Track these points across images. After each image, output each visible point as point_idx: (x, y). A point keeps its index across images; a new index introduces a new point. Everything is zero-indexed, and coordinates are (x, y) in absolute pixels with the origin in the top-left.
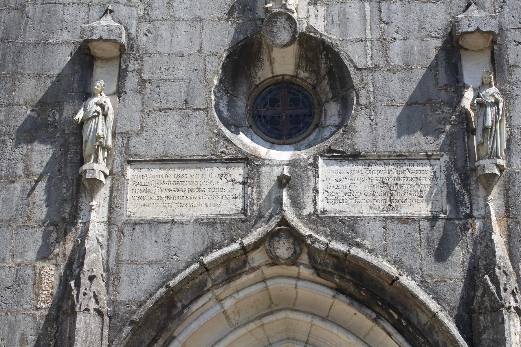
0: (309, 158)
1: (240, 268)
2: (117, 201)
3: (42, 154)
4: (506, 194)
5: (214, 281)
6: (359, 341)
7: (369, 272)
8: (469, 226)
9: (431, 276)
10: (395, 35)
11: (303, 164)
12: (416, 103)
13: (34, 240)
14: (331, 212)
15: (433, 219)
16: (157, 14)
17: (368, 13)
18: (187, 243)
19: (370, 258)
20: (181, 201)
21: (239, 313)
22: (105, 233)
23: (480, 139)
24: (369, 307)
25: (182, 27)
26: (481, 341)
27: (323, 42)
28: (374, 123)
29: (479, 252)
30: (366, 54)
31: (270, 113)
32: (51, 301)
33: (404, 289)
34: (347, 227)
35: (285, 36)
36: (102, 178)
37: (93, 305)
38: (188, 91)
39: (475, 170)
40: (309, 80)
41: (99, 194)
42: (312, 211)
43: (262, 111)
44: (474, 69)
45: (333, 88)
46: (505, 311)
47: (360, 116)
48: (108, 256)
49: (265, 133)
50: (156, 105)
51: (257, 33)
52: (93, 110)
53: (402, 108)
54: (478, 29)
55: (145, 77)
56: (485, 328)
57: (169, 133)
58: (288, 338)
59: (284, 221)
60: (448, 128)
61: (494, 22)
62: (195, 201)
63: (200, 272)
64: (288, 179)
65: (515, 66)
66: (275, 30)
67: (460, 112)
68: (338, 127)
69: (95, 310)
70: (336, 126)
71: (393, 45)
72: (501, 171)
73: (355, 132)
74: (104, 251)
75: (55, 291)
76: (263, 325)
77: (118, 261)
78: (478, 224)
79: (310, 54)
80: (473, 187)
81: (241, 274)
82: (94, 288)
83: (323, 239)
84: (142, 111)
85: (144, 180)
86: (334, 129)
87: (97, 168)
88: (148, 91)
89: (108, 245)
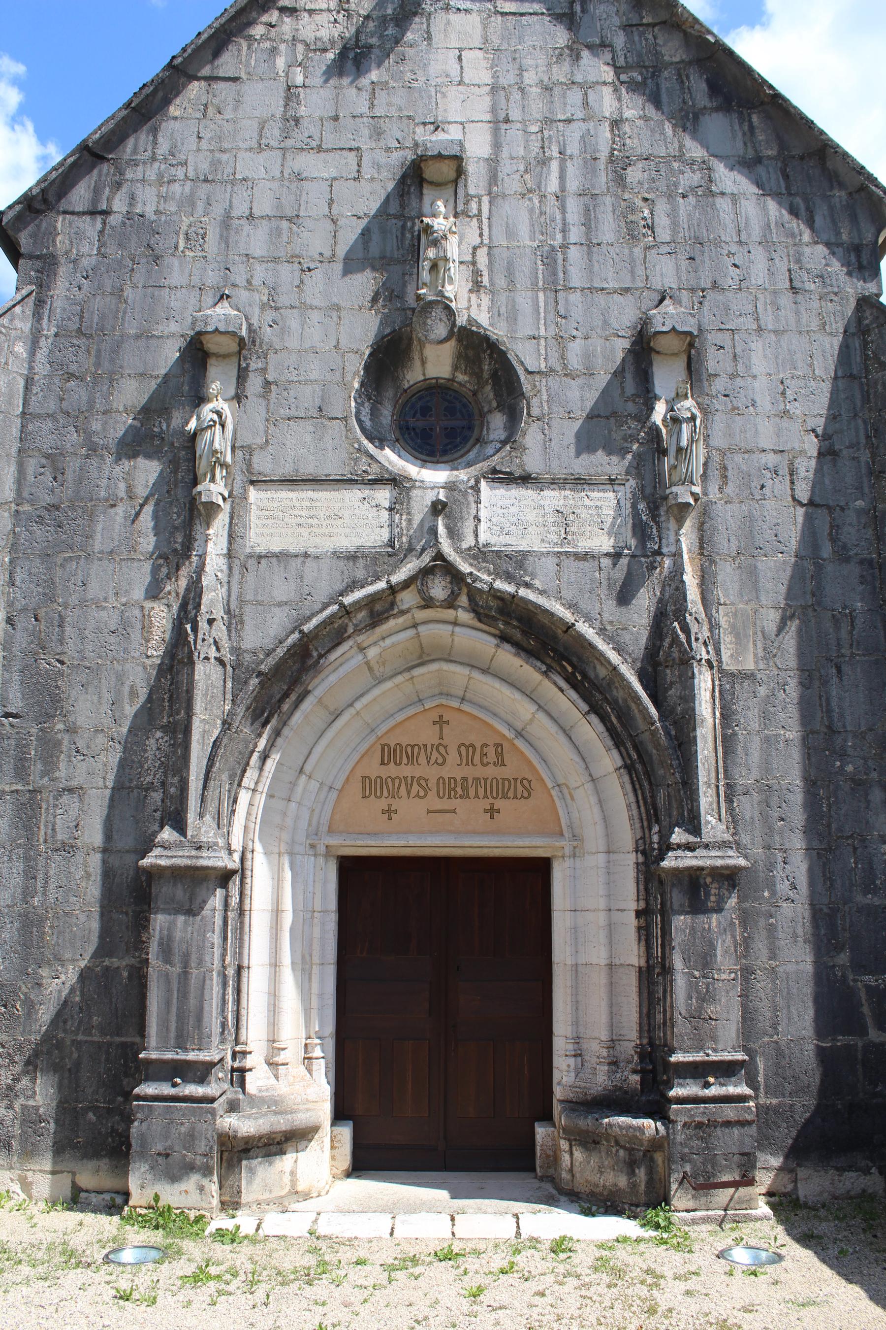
0: (469, 480)
1: (387, 611)
2: (239, 530)
3: (147, 471)
4: (701, 528)
5: (356, 626)
6: (525, 698)
7: (540, 617)
8: (656, 564)
9: (611, 622)
10: (575, 333)
11: (462, 487)
12: (599, 416)
14: (495, 545)
15: (616, 556)
16: (283, 300)
17: (542, 304)
18: (324, 582)
19: (541, 601)
20: (314, 530)
21: (384, 664)
22: (225, 568)
23: (673, 461)
24: (538, 658)
25: (315, 316)
26: (666, 698)
27: (487, 338)
29: (667, 595)
30: (539, 355)
31: (420, 424)
32: (163, 648)
33: (581, 638)
34: (514, 563)
35: (441, 330)
36: (221, 502)
37: (213, 653)
38: (322, 396)
40: (468, 385)
41: (216, 521)
42: (473, 544)
43: (412, 422)
44: (667, 377)
46: (695, 664)
47: (531, 430)
48: (229, 596)
49: (414, 449)
51: (407, 326)
52: (208, 419)
53: (581, 421)
54: (674, 329)
55: (270, 379)
56: (672, 683)
57: (299, 447)
58: (441, 694)
59: (439, 556)
60: (635, 447)
61: (693, 321)
62: (332, 530)
63: (340, 615)
64: (444, 505)
65: (715, 375)
66: (429, 322)
67: (650, 428)
68: (504, 443)
69: (216, 658)
70: (501, 442)
71: (571, 344)
72: (696, 500)
73: (525, 449)
74: (225, 589)
75: (167, 636)
76: (412, 678)
77: (241, 601)
78: (667, 562)
80: (662, 519)
81: (388, 618)
82: (214, 633)
83: (485, 577)
84: (267, 420)
85: (270, 505)
86: (499, 445)
87: (214, 489)
88: (273, 395)
89: (229, 582)
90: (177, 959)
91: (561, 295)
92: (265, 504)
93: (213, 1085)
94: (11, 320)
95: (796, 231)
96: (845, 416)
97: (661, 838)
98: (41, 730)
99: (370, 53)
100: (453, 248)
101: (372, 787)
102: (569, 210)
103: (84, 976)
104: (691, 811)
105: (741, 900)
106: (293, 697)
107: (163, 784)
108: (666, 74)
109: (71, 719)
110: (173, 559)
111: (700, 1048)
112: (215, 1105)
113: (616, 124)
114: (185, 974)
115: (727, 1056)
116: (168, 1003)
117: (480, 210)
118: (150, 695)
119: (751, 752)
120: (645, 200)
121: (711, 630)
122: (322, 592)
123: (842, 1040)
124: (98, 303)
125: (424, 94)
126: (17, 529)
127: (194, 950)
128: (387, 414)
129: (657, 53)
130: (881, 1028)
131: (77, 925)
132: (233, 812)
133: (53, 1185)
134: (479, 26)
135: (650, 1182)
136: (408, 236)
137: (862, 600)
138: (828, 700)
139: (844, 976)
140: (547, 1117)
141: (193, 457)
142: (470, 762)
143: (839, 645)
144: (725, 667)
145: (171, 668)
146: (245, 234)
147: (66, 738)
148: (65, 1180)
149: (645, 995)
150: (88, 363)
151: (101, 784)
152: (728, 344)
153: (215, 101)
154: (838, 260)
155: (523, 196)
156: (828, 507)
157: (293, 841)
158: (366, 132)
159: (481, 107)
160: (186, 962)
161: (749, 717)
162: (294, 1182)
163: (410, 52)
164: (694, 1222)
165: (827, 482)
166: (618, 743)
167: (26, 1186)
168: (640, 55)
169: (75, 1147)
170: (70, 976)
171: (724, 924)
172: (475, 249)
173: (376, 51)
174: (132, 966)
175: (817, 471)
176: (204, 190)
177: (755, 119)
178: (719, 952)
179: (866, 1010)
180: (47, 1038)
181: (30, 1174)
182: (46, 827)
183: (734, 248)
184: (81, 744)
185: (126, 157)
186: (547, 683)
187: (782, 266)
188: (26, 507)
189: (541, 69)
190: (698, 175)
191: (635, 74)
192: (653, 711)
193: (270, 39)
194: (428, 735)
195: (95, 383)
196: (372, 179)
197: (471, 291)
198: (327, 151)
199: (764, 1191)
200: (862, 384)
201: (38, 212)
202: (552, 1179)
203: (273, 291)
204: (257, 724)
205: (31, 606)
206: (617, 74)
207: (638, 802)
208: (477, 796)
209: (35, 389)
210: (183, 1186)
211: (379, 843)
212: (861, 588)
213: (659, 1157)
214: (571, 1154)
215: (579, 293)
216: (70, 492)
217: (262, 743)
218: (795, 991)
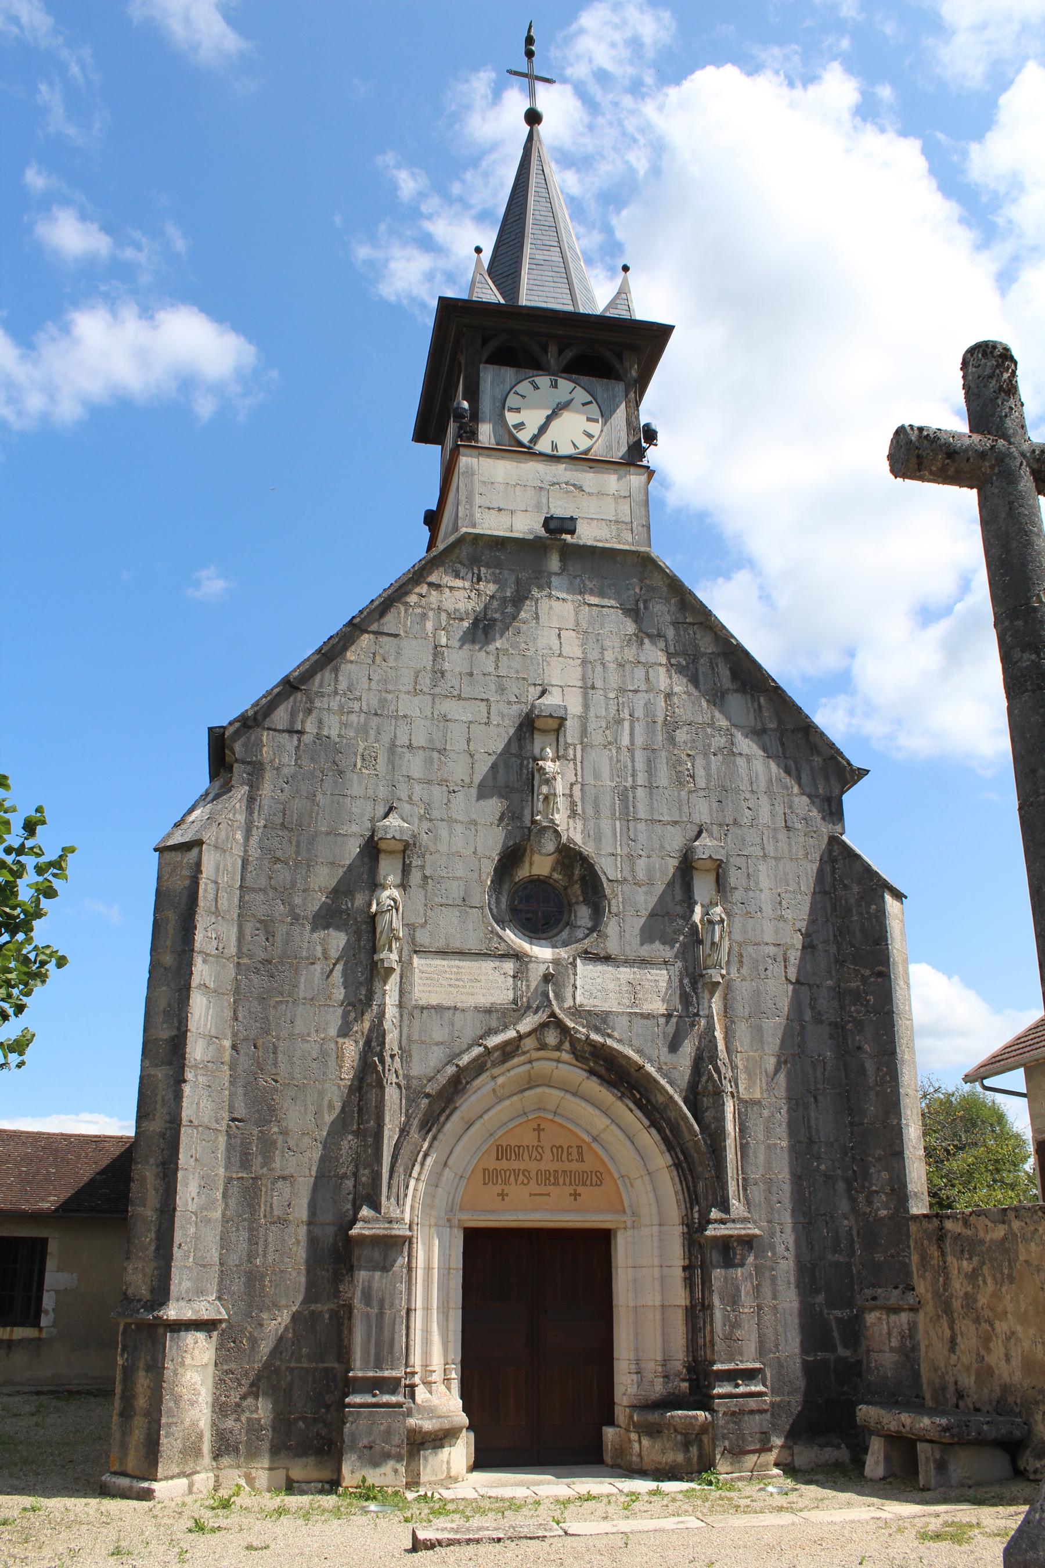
1: (514, 1051)
3: (338, 940)
4: (725, 998)
9: (666, 1063)
10: (641, 853)
11: (564, 963)
12: (657, 915)
13: (334, 1019)
15: (668, 1016)
16: (435, 814)
17: (618, 830)
18: (469, 1027)
19: (615, 1045)
22: (397, 1015)
23: (708, 951)
24: (615, 1087)
25: (459, 828)
27: (580, 853)
28: (622, 929)
32: (352, 1072)
33: (648, 1075)
34: (600, 1020)
35: (550, 846)
37: (395, 1080)
39: (702, 976)
44: (703, 888)
45: (584, 892)
54: (710, 857)
55: (428, 874)
56: (708, 1108)
58: (539, 1109)
59: (553, 1015)
60: (681, 938)
61: (723, 852)
68: (592, 930)
75: (355, 1064)
78: (703, 1022)
79: (566, 861)
80: (700, 991)
81: (514, 1057)
86: (587, 932)
87: (391, 957)
88: (430, 886)
90: (375, 1303)
91: (631, 824)
92: (425, 968)
97: (700, 1215)
98: (260, 1131)
99: (495, 625)
100: (560, 787)
101: (490, 1176)
102: (637, 760)
103: (295, 1318)
104: (722, 1196)
105: (756, 1258)
106: (447, 1112)
107: (355, 1175)
108: (702, 661)
109: (284, 1124)
110: (359, 1007)
111: (731, 1360)
113: (668, 696)
114: (381, 1315)
115: (750, 1365)
116: (369, 1335)
117: (575, 756)
119: (759, 1156)
120: (688, 755)
122: (469, 1034)
123: (820, 1355)
124: (296, 804)
126: (239, 977)
127: (387, 1296)
129: (696, 646)
130: (846, 1347)
131: (290, 1280)
132: (406, 1195)
133: (269, 1479)
135: (700, 1456)
136: (525, 771)
138: (808, 1120)
139: (821, 1311)
140: (611, 1422)
143: (816, 1082)
145: (360, 1089)
146: (406, 759)
148: (281, 1474)
149: (690, 1325)
150: (290, 851)
151: (307, 1174)
152: (744, 866)
155: (605, 746)
158: (493, 687)
159: (574, 676)
162: (449, 1469)
163: (524, 627)
165: (808, 967)
166: (670, 1147)
167: (250, 1480)
168: (684, 646)
169: (288, 1448)
170: (284, 1318)
171: (746, 1274)
172: (572, 785)
173: (499, 624)
174: (332, 1310)
175: (801, 959)
176: (374, 721)
177: (762, 700)
178: (743, 1294)
179: (836, 1334)
180: (267, 1365)
181: (254, 1470)
182: (266, 1205)
183: (748, 795)
184: (292, 1143)
185: (315, 689)
186: (619, 1103)
187: (780, 810)
188: (245, 961)
190: (723, 740)
191: (681, 660)
193: (421, 606)
194: (529, 1138)
195: (296, 865)
196: (498, 725)
197: (569, 817)
198: (465, 699)
201: (249, 727)
204: (423, 1132)
205: (251, 1037)
206: (668, 659)
208: (564, 1184)
209: (250, 868)
210: (382, 1470)
211: (497, 1218)
212: (830, 1042)
213: (705, 1438)
214: (640, 1442)
215: (643, 823)
216: (279, 950)
217: (426, 1145)
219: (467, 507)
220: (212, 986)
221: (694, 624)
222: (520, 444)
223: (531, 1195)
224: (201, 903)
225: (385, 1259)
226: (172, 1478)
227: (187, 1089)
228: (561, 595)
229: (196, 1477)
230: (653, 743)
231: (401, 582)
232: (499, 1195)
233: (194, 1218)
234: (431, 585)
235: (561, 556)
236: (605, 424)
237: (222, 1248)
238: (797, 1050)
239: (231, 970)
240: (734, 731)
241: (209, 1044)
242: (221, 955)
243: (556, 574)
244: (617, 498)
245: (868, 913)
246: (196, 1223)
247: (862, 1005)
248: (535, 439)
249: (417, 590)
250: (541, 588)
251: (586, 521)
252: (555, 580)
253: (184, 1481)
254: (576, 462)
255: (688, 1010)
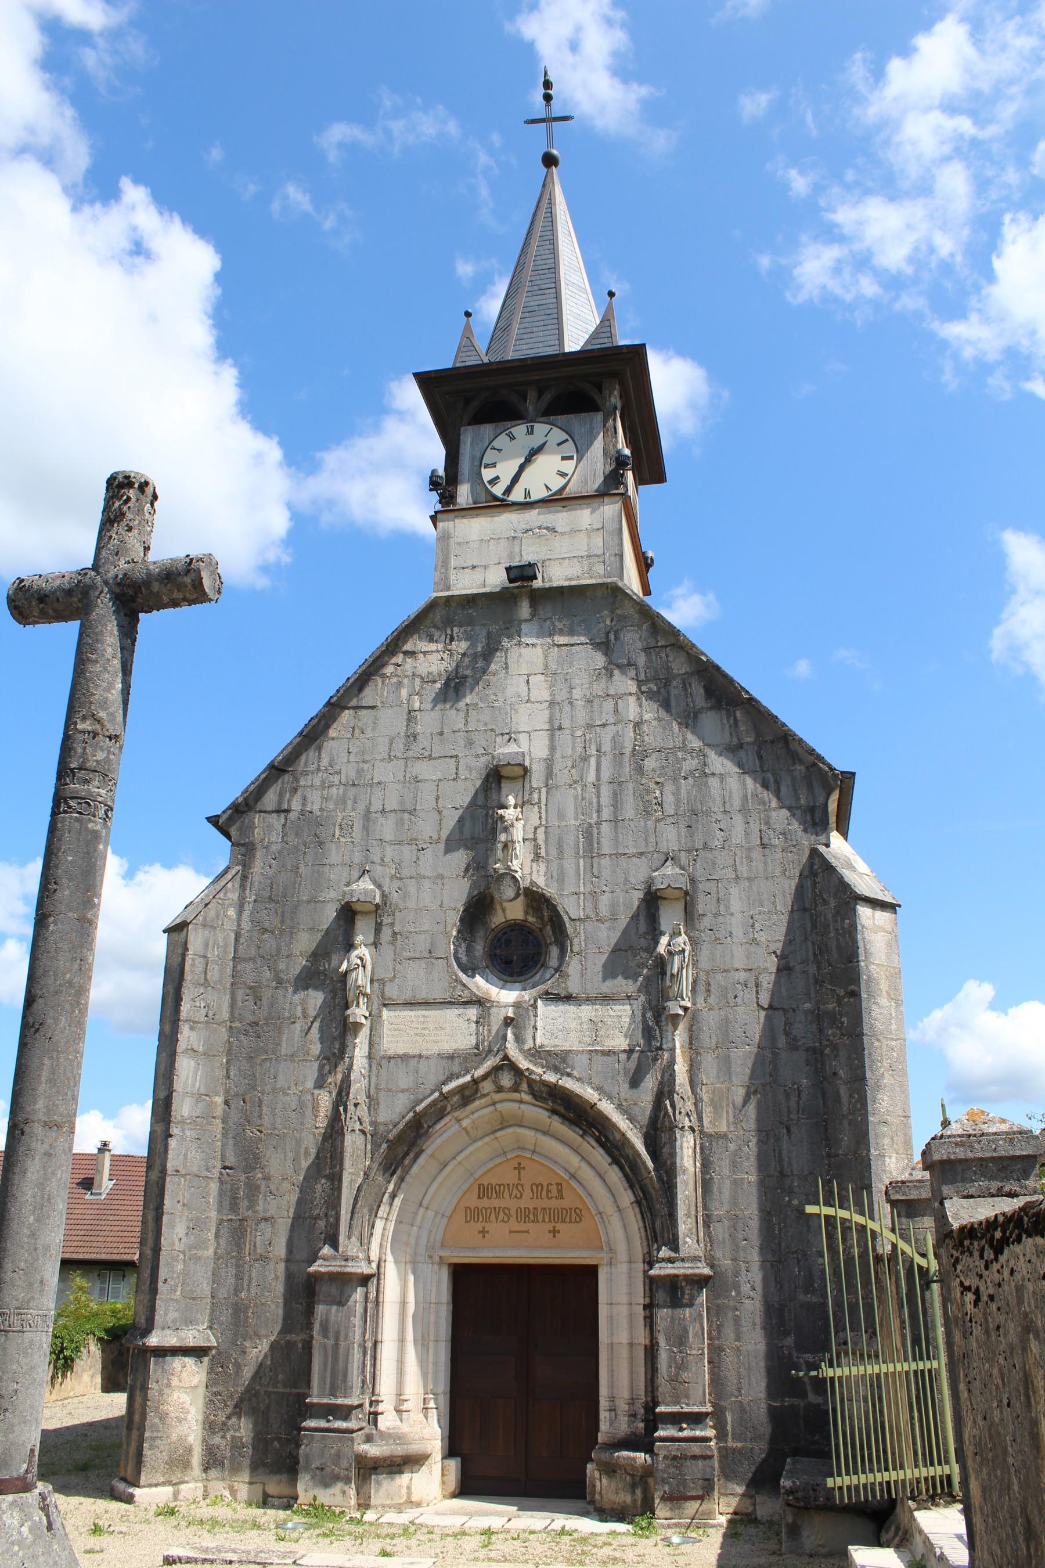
1: (473, 1095)
2: (376, 1039)
3: (316, 999)
6: (572, 1151)
9: (626, 1100)
10: (605, 888)
12: (620, 950)
13: (311, 1072)
15: (630, 1052)
16: (405, 872)
17: (582, 868)
18: (431, 1074)
22: (367, 1066)
24: (577, 1125)
25: (427, 884)
26: (661, 1154)
27: (543, 895)
28: (583, 968)
32: (326, 1121)
34: (559, 1060)
35: (510, 893)
36: (363, 1021)
37: (357, 1126)
39: (664, 1008)
43: (498, 952)
44: (670, 917)
45: (554, 933)
46: (677, 1130)
50: (407, 954)
57: (418, 979)
59: (506, 1057)
60: (645, 971)
64: (512, 1019)
68: (557, 970)
75: (329, 1113)
77: (378, 1089)
78: (666, 1055)
79: (535, 904)
81: (474, 1100)
82: (358, 1113)
87: (359, 1012)
88: (399, 942)
90: (331, 1335)
91: (595, 860)
93: (353, 1421)
94: (225, 894)
95: (767, 799)
96: (798, 940)
100: (518, 833)
101: (472, 1214)
103: (273, 1346)
104: (674, 1235)
106: (412, 1155)
107: (326, 1215)
108: (674, 683)
111: (677, 1402)
112: (354, 1435)
113: (637, 725)
114: (336, 1345)
115: (696, 1409)
116: (325, 1365)
117: (540, 799)
118: (318, 1154)
119: (723, 1191)
120: (657, 783)
121: (695, 1104)
122: (432, 1080)
123: (788, 1401)
125: (502, 711)
128: (479, 948)
132: (372, 1234)
134: (542, 656)
136: (490, 821)
137: (807, 1078)
139: (790, 1354)
141: (344, 989)
142: (539, 1197)
144: (706, 1130)
147: (263, 1183)
148: (259, 1488)
150: (276, 921)
151: (286, 1215)
152: (713, 891)
153: (360, 724)
154: (797, 820)
156: (783, 1009)
157: (415, 1254)
158: (462, 743)
159: (541, 718)
160: (337, 1337)
161: (722, 1167)
162: (409, 1494)
164: (669, 1526)
165: (783, 990)
166: (632, 1187)
167: (233, 1492)
168: (656, 671)
169: (265, 1465)
170: (264, 1346)
173: (470, 680)
174: (305, 1340)
175: (775, 983)
176: (353, 790)
177: (738, 714)
178: (691, 1335)
180: (249, 1389)
181: (236, 1484)
184: (273, 1187)
187: (755, 827)
189: (584, 686)
190: (696, 761)
192: (650, 1165)
193: (397, 676)
194: (510, 1178)
195: (281, 935)
196: (466, 779)
199: (731, 1511)
200: (811, 915)
201: (243, 812)
202: (592, 1502)
203: (399, 865)
204: (387, 1174)
206: (639, 687)
207: (645, 1227)
208: (544, 1221)
209: (242, 940)
212: (807, 1068)
213: (651, 1481)
215: (608, 858)
218: (753, 1364)
219: (443, 570)
220: (201, 1049)
221: (666, 647)
222: (495, 498)
223: (511, 1232)
224: (188, 976)
225: (341, 1295)
226: (156, 1485)
227: (173, 1143)
228: (530, 641)
229: (183, 1487)
230: (619, 775)
231: (375, 656)
232: (479, 1232)
233: (182, 1256)
234: (406, 653)
235: (531, 602)
236: (579, 461)
237: (214, 1282)
238: (768, 1079)
239: (223, 1033)
240: (708, 751)
241: (197, 1101)
242: (210, 1020)
243: (526, 621)
244: (589, 532)
245: (843, 928)
246: (184, 1261)
247: (838, 1028)
248: (508, 490)
249: (394, 660)
250: (510, 637)
251: (558, 562)
252: (523, 626)
253: (170, 1489)
254: (549, 505)
255: (650, 1044)
